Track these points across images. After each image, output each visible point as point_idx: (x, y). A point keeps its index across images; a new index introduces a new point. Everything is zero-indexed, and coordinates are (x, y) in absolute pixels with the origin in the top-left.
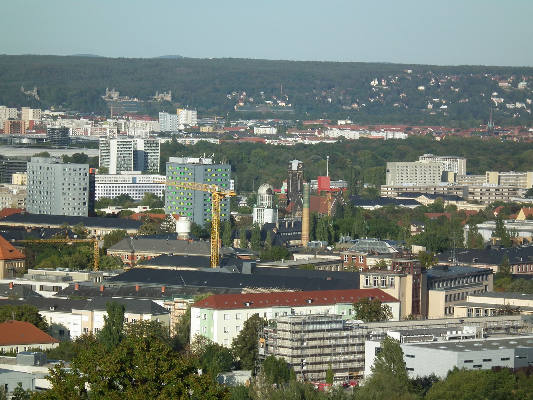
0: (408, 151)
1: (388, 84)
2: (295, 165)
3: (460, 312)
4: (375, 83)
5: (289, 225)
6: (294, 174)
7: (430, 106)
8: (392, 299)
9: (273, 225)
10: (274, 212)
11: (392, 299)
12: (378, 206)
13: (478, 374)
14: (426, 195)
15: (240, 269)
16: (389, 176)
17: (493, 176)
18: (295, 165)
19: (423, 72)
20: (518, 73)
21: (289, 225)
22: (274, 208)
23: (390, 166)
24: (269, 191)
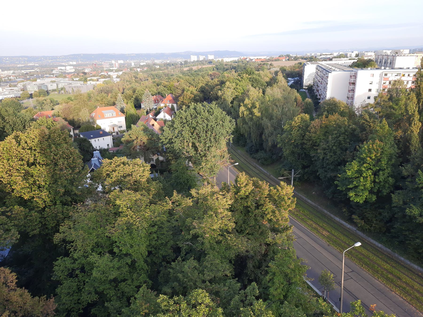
3: (5, 90)
13: (9, 98)
17: (6, 72)
20: (6, 57)
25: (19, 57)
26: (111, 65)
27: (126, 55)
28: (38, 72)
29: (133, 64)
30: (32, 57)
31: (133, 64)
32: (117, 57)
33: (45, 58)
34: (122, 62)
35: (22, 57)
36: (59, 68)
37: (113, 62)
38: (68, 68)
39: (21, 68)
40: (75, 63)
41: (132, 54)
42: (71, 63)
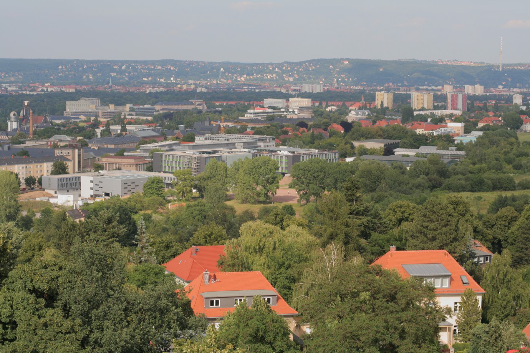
0: (75, 97)
1: (66, 68)
2: (26, 103)
4: (60, 67)
5: (24, 129)
6: (26, 107)
7: (85, 77)
8: (68, 160)
9: (17, 129)
10: (18, 123)
11: (68, 160)
12: (63, 121)
14: (83, 115)
15: (3, 149)
16: (67, 107)
18: (26, 103)
19: (81, 63)
20: (123, 62)
21: (24, 129)
22: (17, 121)
23: (67, 103)
24: (14, 115)
25: (154, 63)
26: (440, 100)
27: (498, 67)
28: (200, 112)
29: (518, 100)
30: (191, 63)
31: (518, 100)
32: (462, 75)
33: (232, 68)
34: (479, 90)
35: (164, 63)
36: (269, 102)
37: (448, 90)
38: (296, 103)
39: (156, 98)
40: (318, 89)
41: (519, 64)
42: (306, 88)
